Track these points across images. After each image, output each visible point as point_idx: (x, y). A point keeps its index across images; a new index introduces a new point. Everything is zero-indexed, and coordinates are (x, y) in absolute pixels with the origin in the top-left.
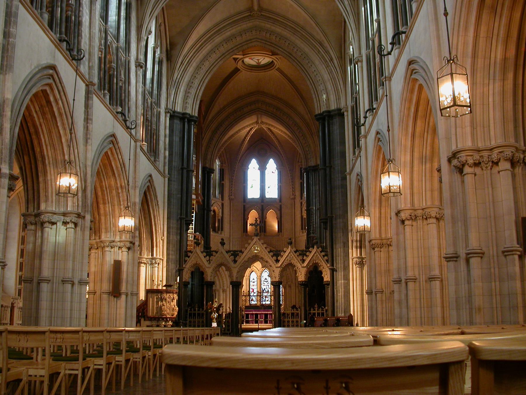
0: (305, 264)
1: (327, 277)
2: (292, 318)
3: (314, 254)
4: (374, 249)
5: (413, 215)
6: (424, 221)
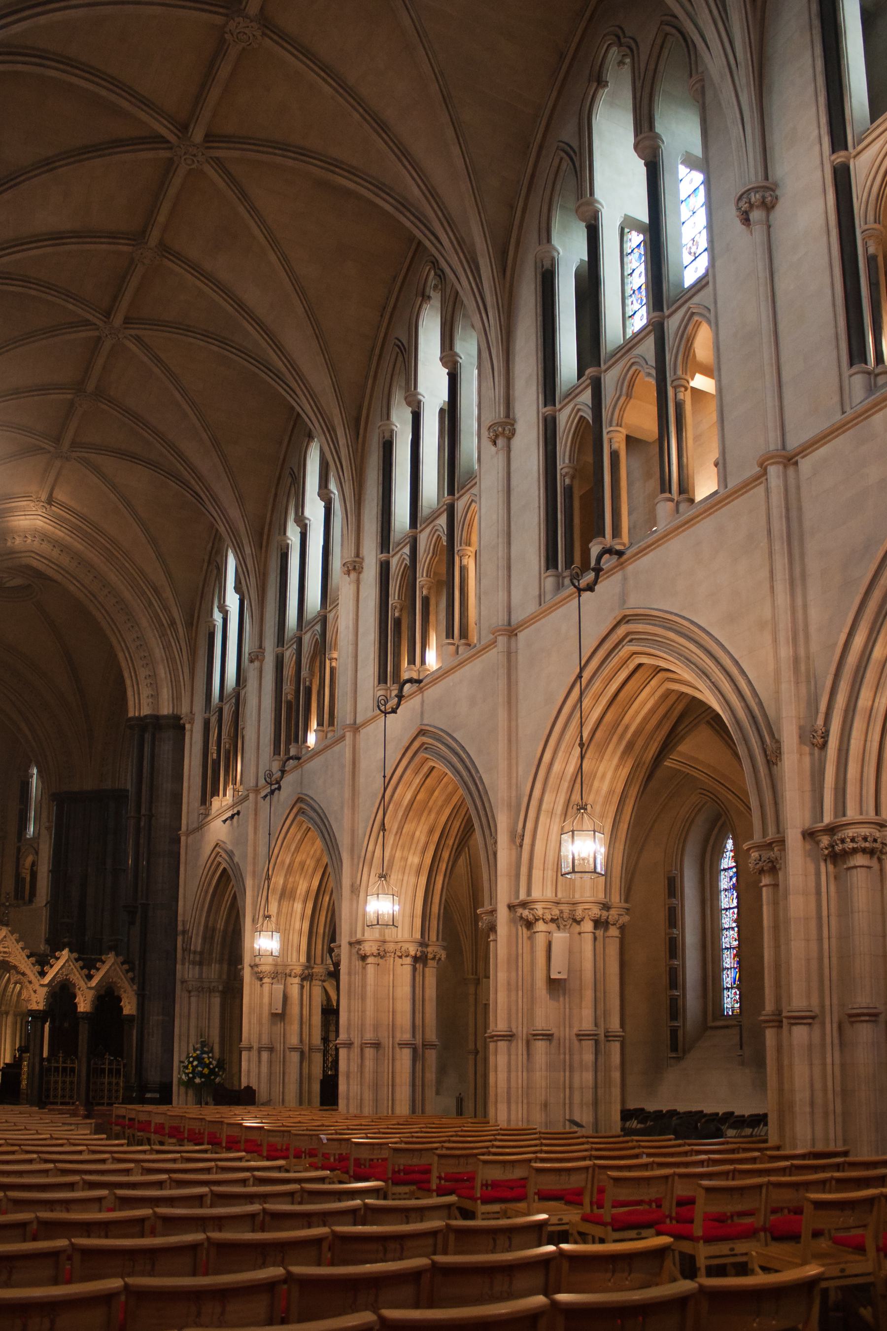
0: (94, 983)
1: (129, 1007)
2: (62, 1077)
3: (111, 967)
4: (261, 979)
5: (382, 949)
6: (397, 959)
